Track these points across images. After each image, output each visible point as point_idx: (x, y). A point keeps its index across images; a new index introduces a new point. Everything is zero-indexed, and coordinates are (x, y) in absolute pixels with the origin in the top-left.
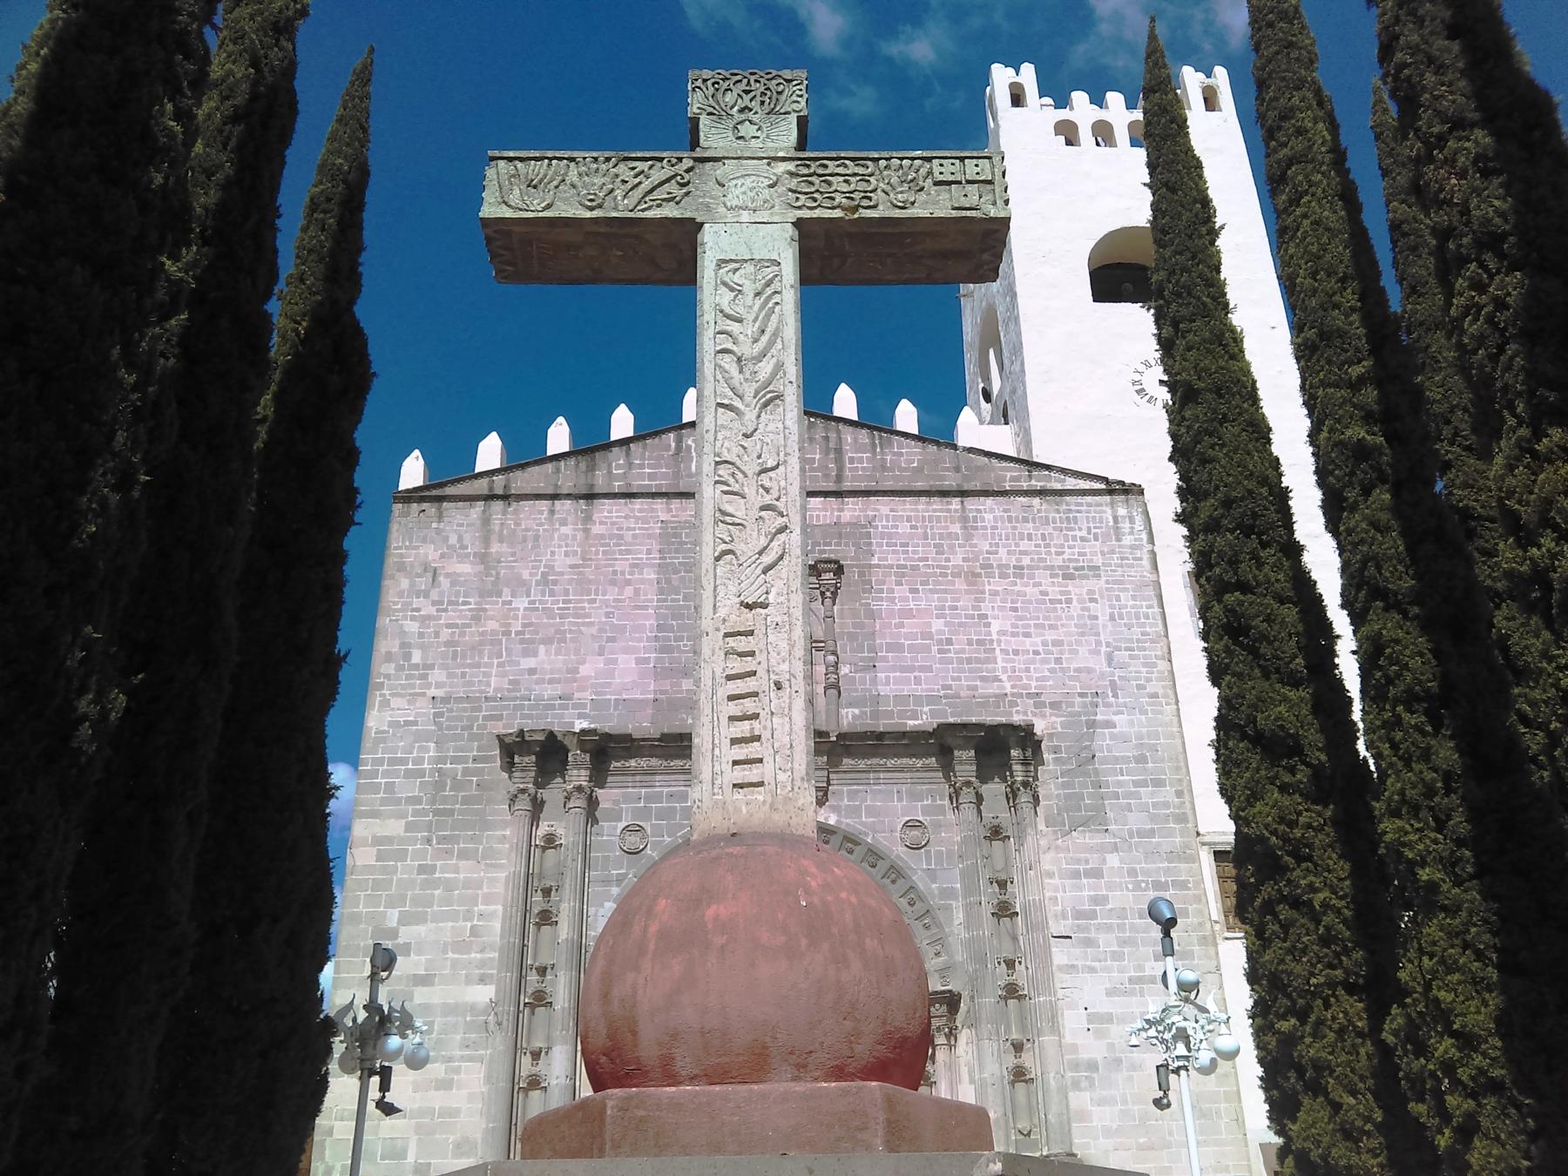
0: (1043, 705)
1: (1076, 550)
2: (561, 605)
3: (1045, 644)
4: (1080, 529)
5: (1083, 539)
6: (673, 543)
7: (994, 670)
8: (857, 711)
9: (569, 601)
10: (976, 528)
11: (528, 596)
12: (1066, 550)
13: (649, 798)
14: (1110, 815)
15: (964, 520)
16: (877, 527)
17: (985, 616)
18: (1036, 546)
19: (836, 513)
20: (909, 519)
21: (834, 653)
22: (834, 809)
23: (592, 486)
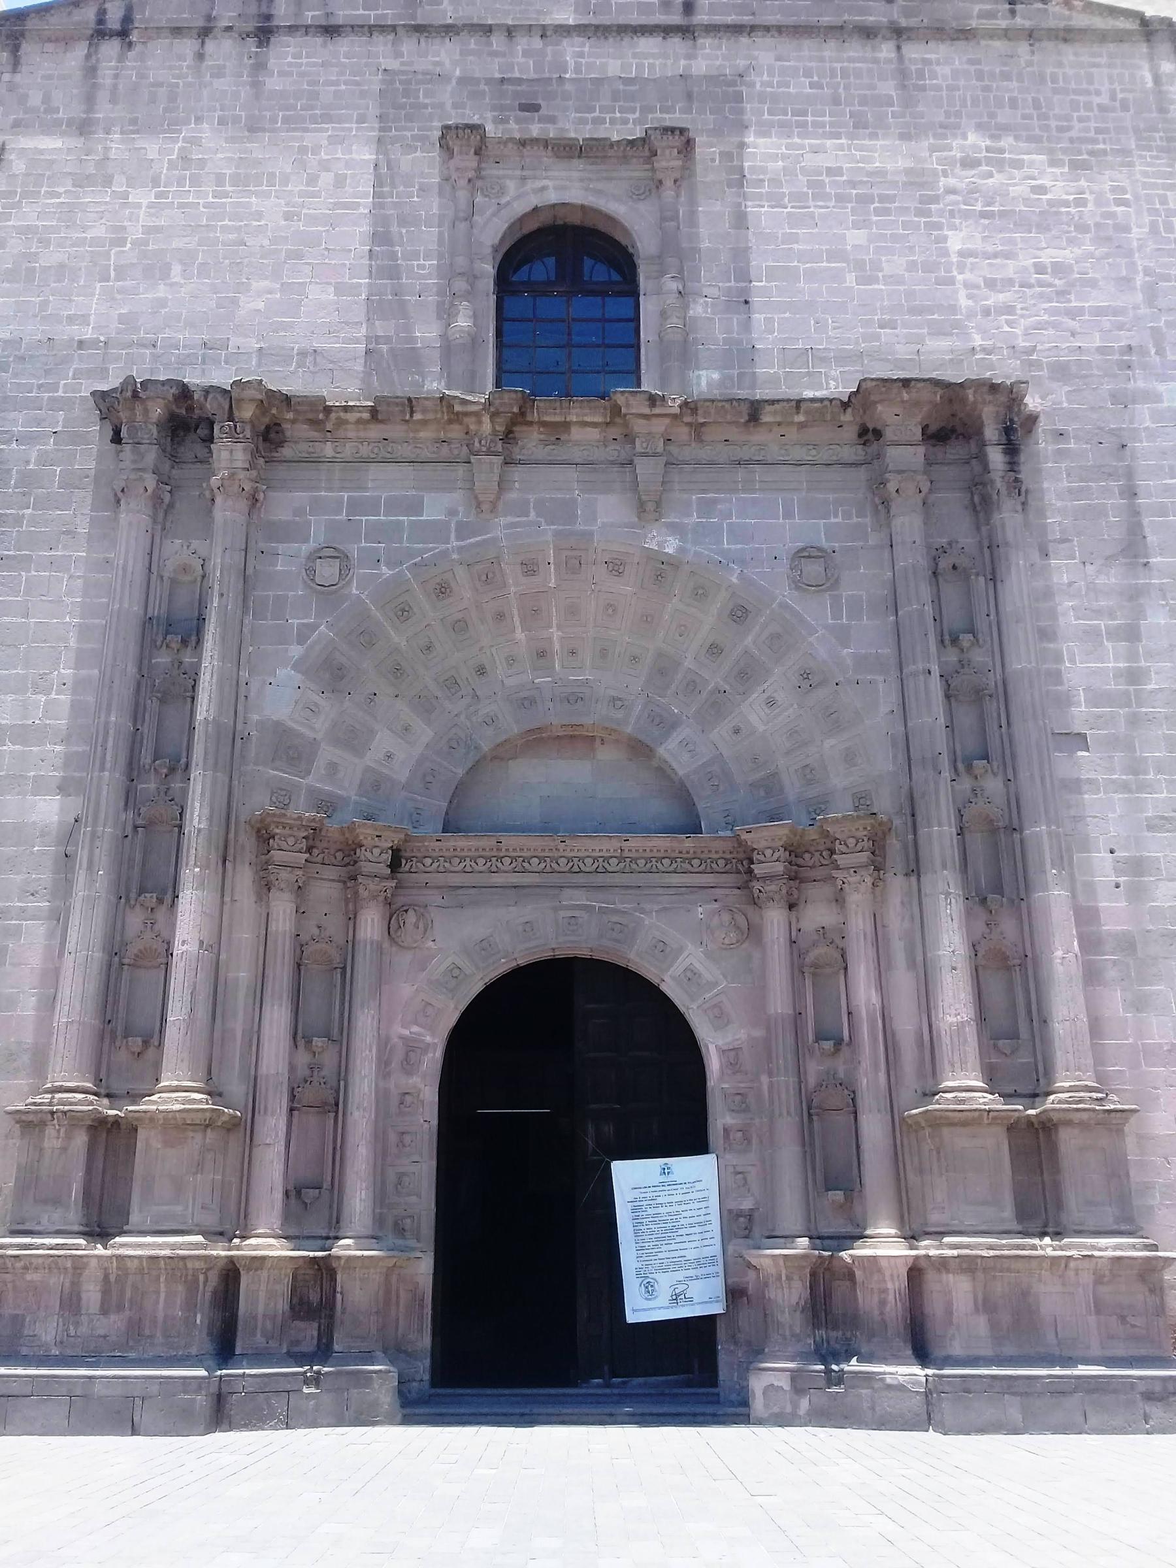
0: (1037, 364)
1: (1093, 124)
2: (211, 199)
3: (1040, 269)
4: (1098, 93)
5: (1102, 108)
6: (403, 107)
7: (954, 309)
8: (716, 376)
9: (226, 195)
10: (923, 88)
11: (156, 182)
12: (1075, 123)
13: (355, 507)
14: (1152, 539)
15: (902, 74)
16: (752, 85)
17: (938, 226)
18: (1024, 117)
19: (683, 62)
20: (808, 73)
21: (680, 277)
22: (676, 529)
23: (268, 17)
